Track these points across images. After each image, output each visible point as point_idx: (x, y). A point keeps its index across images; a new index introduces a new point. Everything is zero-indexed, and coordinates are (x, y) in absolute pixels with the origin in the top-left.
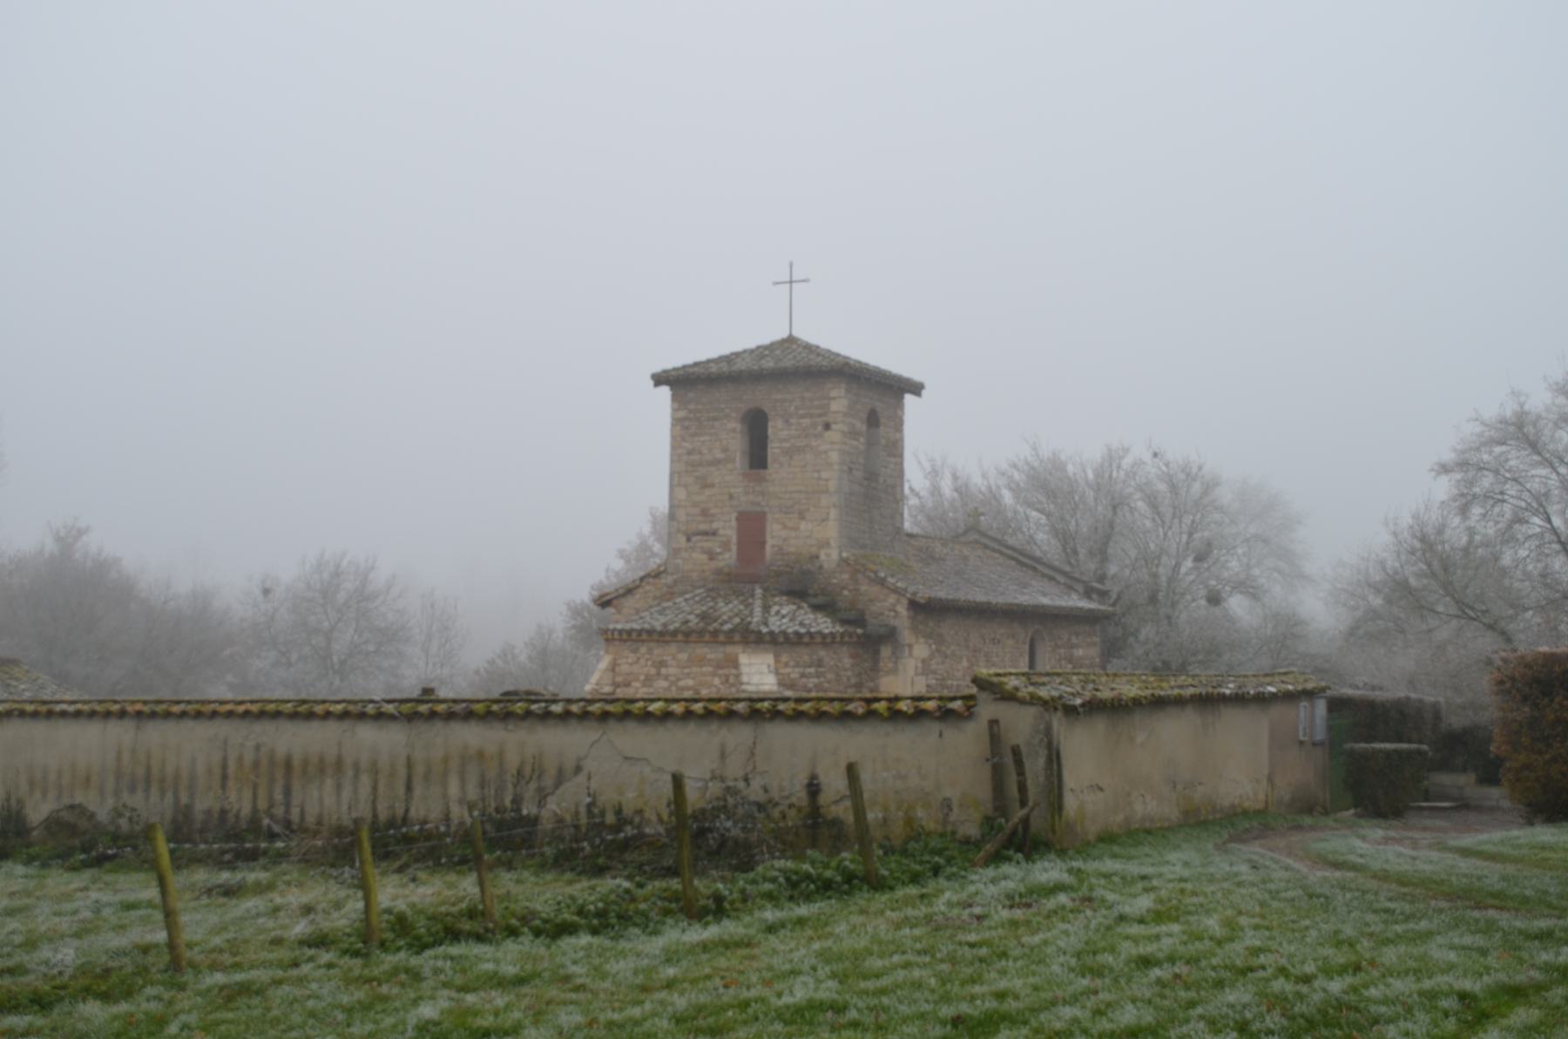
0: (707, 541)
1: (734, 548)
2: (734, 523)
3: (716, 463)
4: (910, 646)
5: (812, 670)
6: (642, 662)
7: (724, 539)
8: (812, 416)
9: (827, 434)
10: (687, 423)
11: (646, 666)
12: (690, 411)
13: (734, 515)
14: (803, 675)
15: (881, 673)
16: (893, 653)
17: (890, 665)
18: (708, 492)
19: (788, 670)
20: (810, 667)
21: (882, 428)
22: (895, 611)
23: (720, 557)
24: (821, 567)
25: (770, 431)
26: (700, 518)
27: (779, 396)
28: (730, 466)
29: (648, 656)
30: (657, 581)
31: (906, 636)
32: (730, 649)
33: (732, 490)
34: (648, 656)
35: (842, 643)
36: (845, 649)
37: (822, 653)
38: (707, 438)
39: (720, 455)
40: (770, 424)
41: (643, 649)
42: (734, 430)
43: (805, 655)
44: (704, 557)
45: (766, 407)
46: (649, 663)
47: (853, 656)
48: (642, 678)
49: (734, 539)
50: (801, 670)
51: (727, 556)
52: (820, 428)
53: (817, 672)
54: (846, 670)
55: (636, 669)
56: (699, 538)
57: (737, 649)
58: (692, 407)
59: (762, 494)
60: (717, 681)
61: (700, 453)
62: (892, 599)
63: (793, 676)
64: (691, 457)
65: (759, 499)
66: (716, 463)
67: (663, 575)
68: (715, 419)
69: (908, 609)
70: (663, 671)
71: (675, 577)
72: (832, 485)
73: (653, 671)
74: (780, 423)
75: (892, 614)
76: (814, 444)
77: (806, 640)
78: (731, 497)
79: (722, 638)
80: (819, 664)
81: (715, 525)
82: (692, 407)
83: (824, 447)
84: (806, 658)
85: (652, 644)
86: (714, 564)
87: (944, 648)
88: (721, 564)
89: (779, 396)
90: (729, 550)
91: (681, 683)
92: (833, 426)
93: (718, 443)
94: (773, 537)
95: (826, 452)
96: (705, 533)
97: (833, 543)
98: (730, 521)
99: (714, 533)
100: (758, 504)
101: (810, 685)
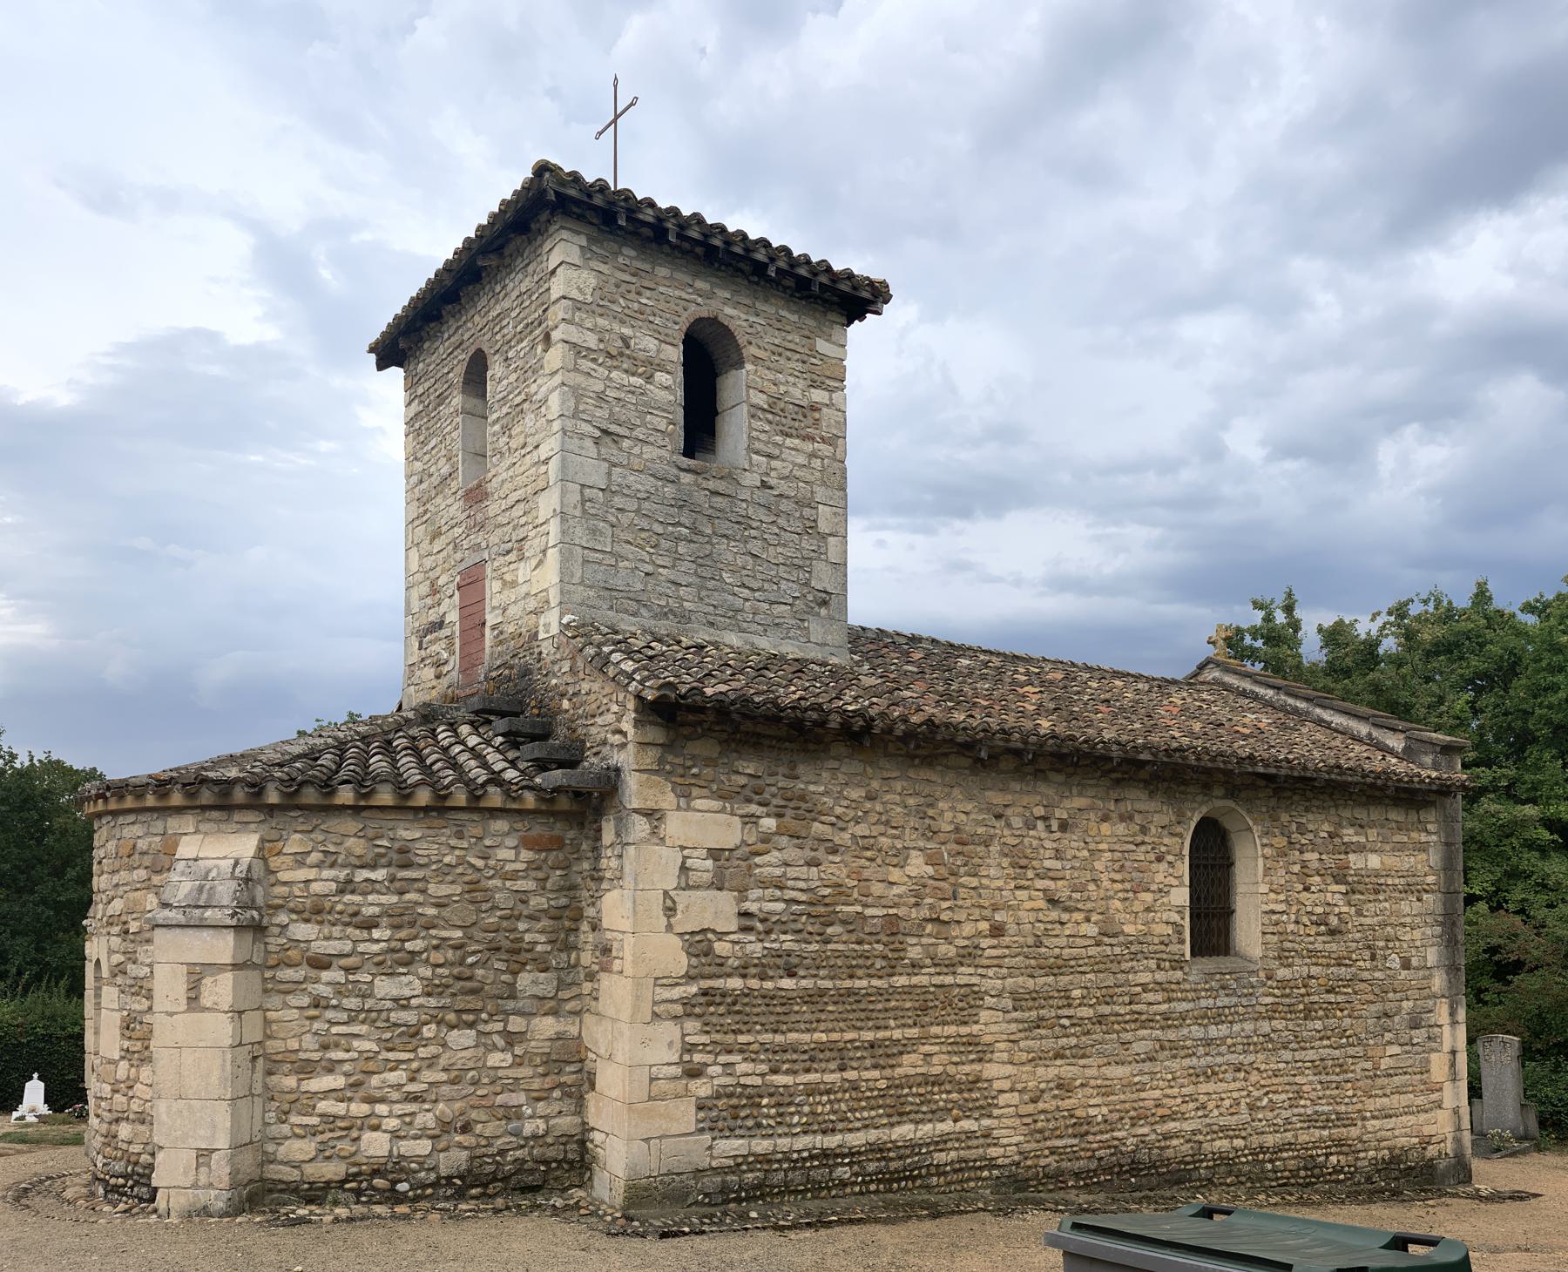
4: (653, 815)
5: (380, 874)
14: (346, 886)
15: (605, 885)
16: (618, 835)
17: (614, 863)
19: (302, 874)
20: (373, 867)
21: (749, 367)
22: (620, 732)
31: (635, 790)
35: (476, 805)
36: (500, 825)
37: (408, 832)
43: (350, 837)
47: (527, 843)
50: (343, 874)
53: (392, 879)
54: (514, 876)
63: (316, 887)
69: (638, 723)
72: (553, 465)
77: (385, 797)
80: (404, 857)
84: (356, 846)
87: (817, 828)
101: (369, 911)
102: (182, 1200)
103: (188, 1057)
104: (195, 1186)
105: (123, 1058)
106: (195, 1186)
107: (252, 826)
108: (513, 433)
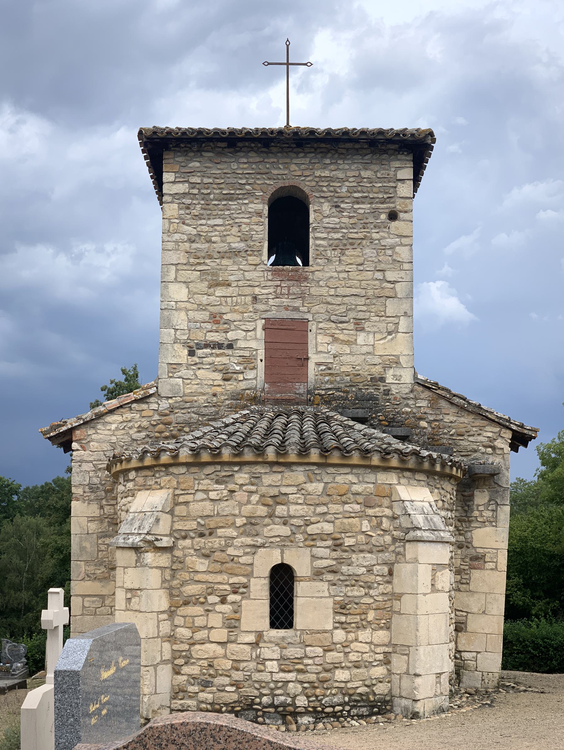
0: (218, 355)
1: (261, 366)
2: (260, 333)
3: (234, 253)
6: (240, 496)
7: (247, 354)
8: (372, 201)
9: (394, 224)
10: (189, 201)
11: (249, 502)
12: (193, 185)
13: (260, 323)
18: (220, 291)
23: (241, 377)
24: (387, 392)
25: (312, 217)
26: (209, 326)
27: (327, 173)
28: (252, 259)
29: (253, 488)
30: (144, 406)
32: (383, 478)
33: (257, 290)
34: (253, 488)
38: (219, 221)
39: (242, 245)
40: (312, 208)
41: (242, 477)
42: (259, 214)
44: (218, 376)
45: (306, 186)
46: (255, 498)
48: (239, 522)
49: (261, 354)
51: (250, 375)
52: (383, 217)
55: (227, 507)
56: (208, 351)
57: (392, 478)
58: (195, 179)
59: (302, 296)
60: (366, 526)
61: (210, 241)
62: (490, 431)
64: (194, 245)
65: (298, 303)
66: (234, 253)
67: (152, 399)
68: (230, 197)
70: (280, 510)
71: (170, 401)
73: (262, 511)
74: (326, 207)
75: (489, 450)
76: (375, 236)
78: (255, 299)
79: (376, 460)
81: (231, 335)
82: (193, 180)
83: (390, 241)
85: (259, 469)
86: (230, 386)
88: (243, 385)
89: (327, 173)
90: (254, 368)
91: (311, 529)
92: (401, 215)
93: (235, 230)
94: (318, 352)
95: (392, 248)
96: (220, 346)
97: (402, 360)
98: (254, 329)
99: (230, 347)
100: (296, 309)
102: (430, 705)
103: (432, 619)
104: (436, 696)
105: (336, 628)
106: (436, 696)
107: (422, 483)
108: (347, 252)
